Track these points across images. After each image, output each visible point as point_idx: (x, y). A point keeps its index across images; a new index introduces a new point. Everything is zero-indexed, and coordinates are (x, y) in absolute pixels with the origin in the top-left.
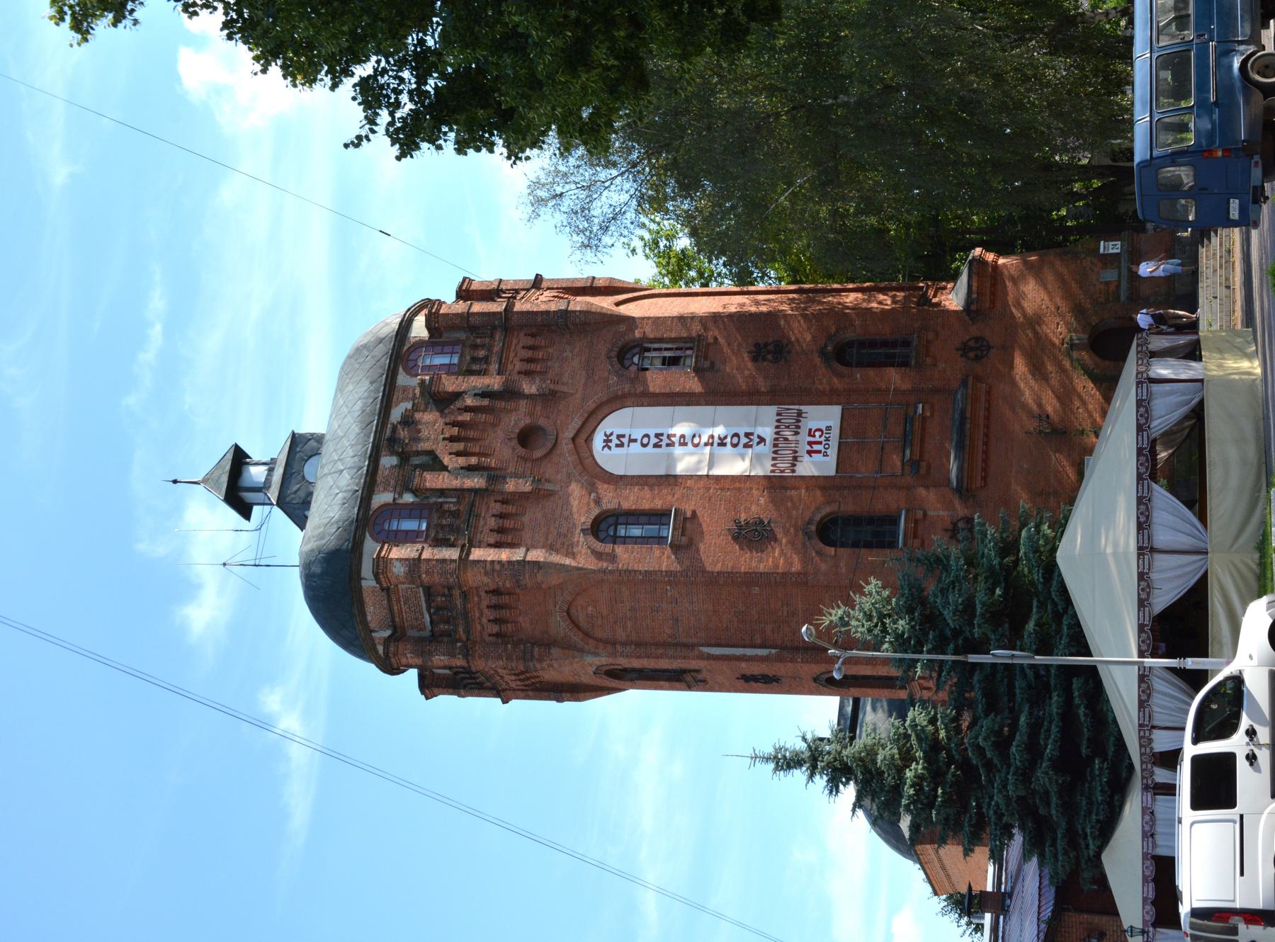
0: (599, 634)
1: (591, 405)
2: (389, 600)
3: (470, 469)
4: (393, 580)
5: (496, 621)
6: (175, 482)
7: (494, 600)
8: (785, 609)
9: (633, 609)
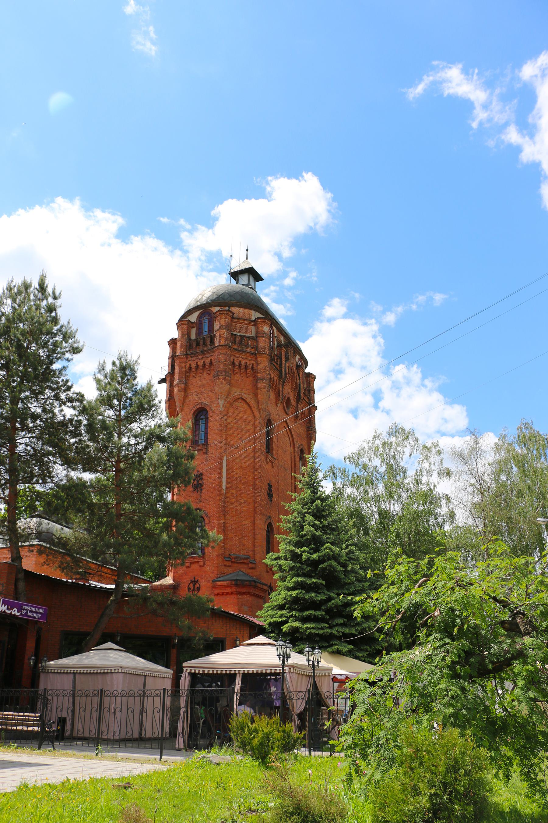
0: (230, 410)
1: (293, 433)
2: (247, 320)
3: (286, 373)
4: (260, 325)
5: (240, 365)
6: (247, 250)
7: (250, 366)
8: (243, 501)
9: (242, 429)
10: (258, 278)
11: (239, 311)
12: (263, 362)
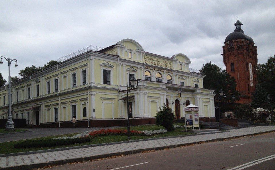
10: (241, 24)
11: (239, 40)
12: (245, 51)
